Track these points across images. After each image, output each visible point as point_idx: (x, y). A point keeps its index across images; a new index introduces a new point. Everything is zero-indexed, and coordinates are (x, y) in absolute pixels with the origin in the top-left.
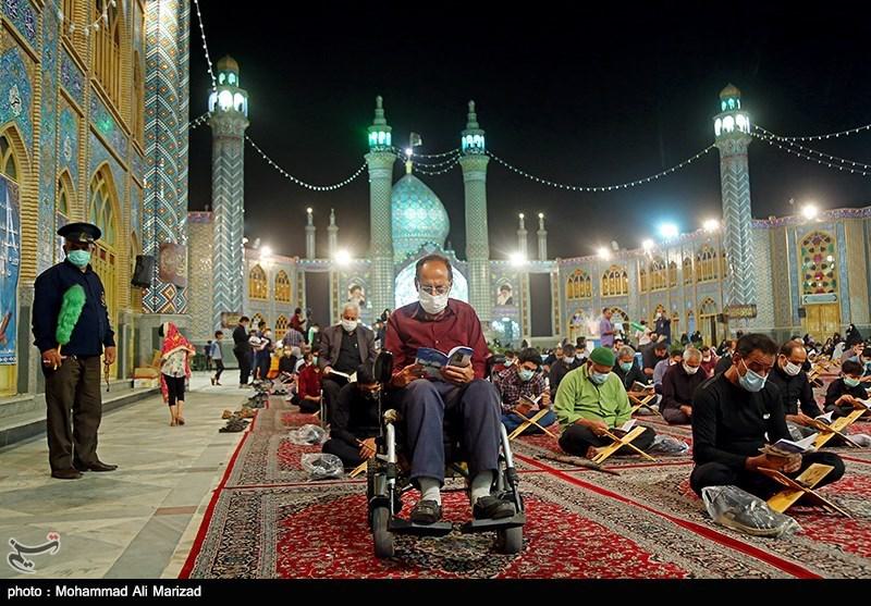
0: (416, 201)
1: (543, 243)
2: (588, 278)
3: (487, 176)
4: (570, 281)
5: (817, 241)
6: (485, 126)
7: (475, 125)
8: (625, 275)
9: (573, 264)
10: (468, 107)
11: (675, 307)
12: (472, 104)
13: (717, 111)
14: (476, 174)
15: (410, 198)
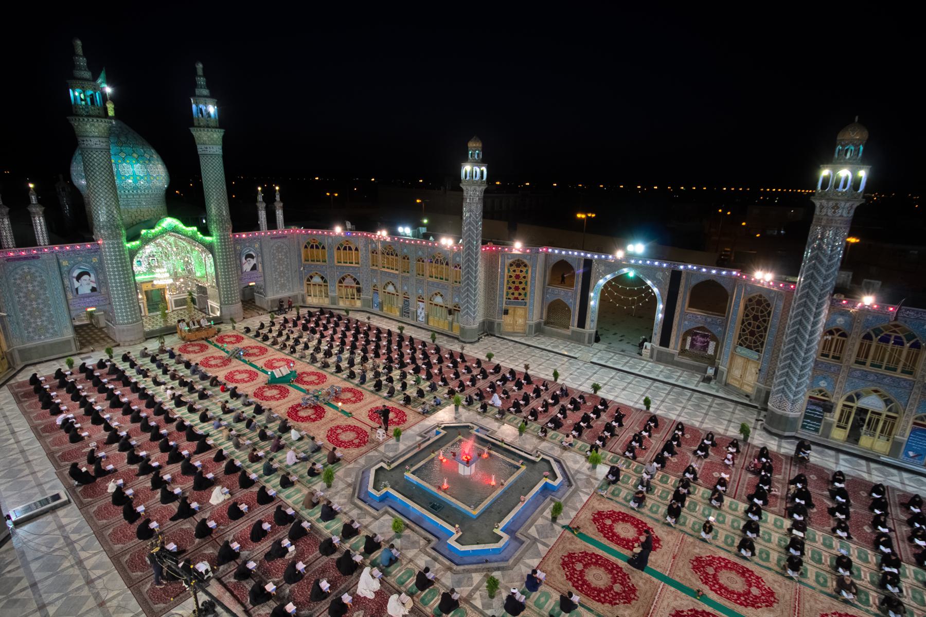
0: (128, 155)
1: (280, 214)
2: (323, 248)
3: (224, 148)
4: (306, 247)
5: (518, 266)
6: (216, 95)
7: (205, 92)
8: (356, 249)
9: (308, 234)
10: (195, 69)
11: (406, 288)
12: (200, 66)
13: (465, 159)
14: (210, 144)
15: (121, 151)
